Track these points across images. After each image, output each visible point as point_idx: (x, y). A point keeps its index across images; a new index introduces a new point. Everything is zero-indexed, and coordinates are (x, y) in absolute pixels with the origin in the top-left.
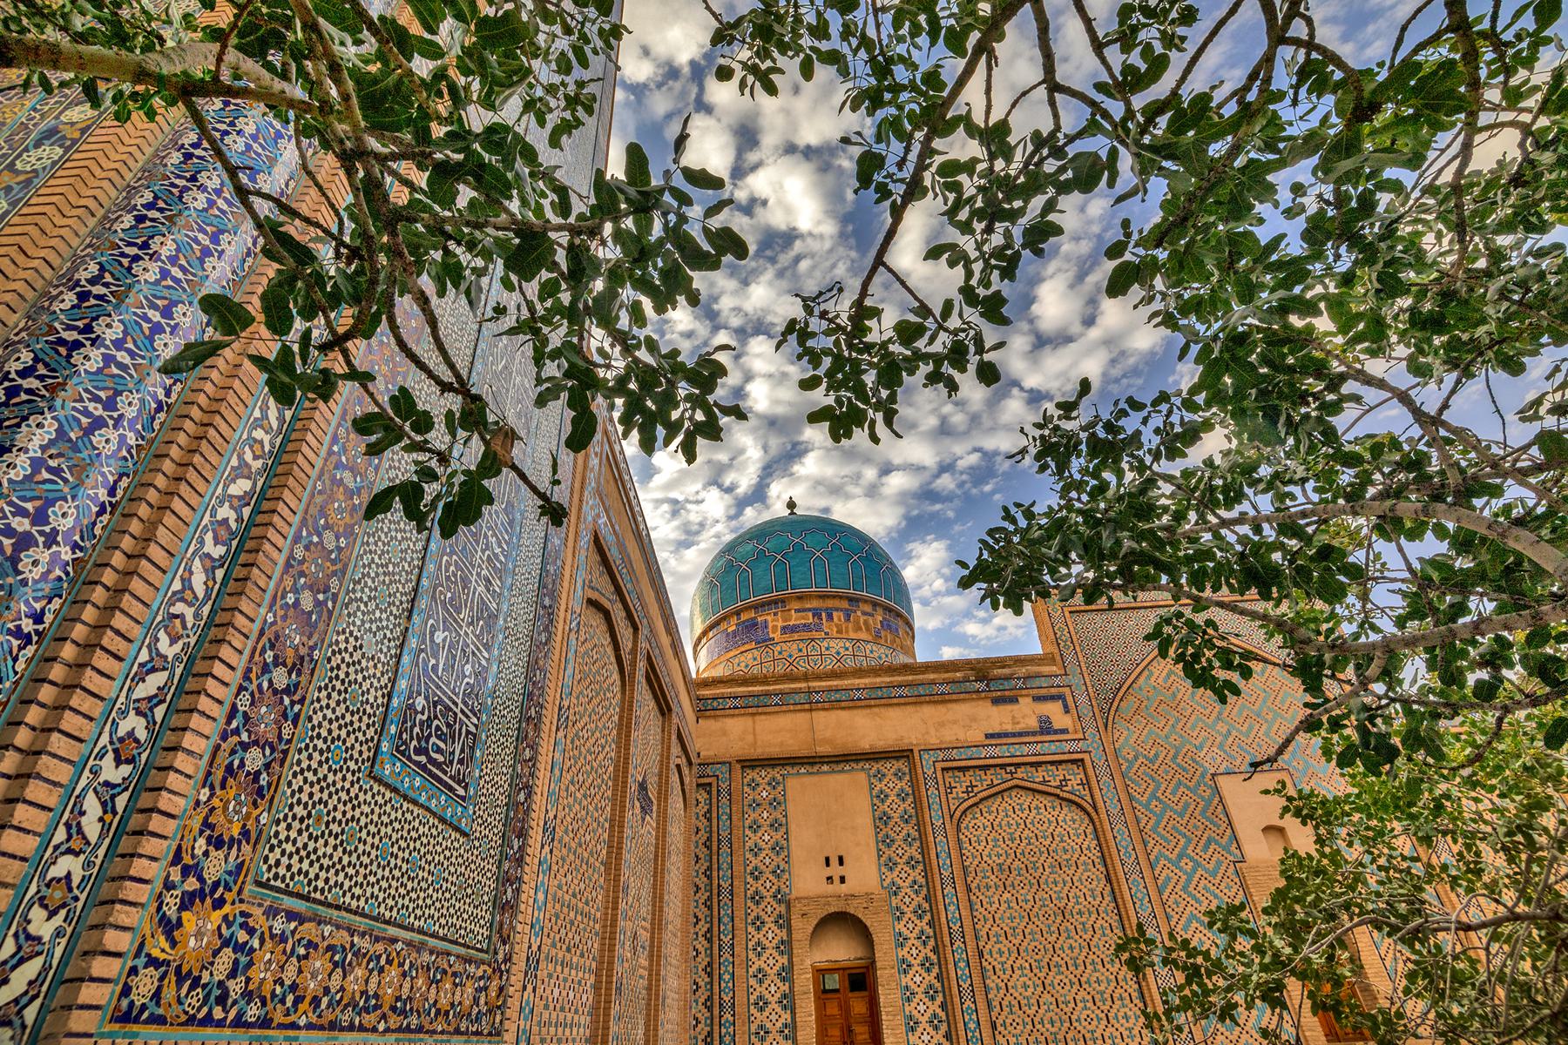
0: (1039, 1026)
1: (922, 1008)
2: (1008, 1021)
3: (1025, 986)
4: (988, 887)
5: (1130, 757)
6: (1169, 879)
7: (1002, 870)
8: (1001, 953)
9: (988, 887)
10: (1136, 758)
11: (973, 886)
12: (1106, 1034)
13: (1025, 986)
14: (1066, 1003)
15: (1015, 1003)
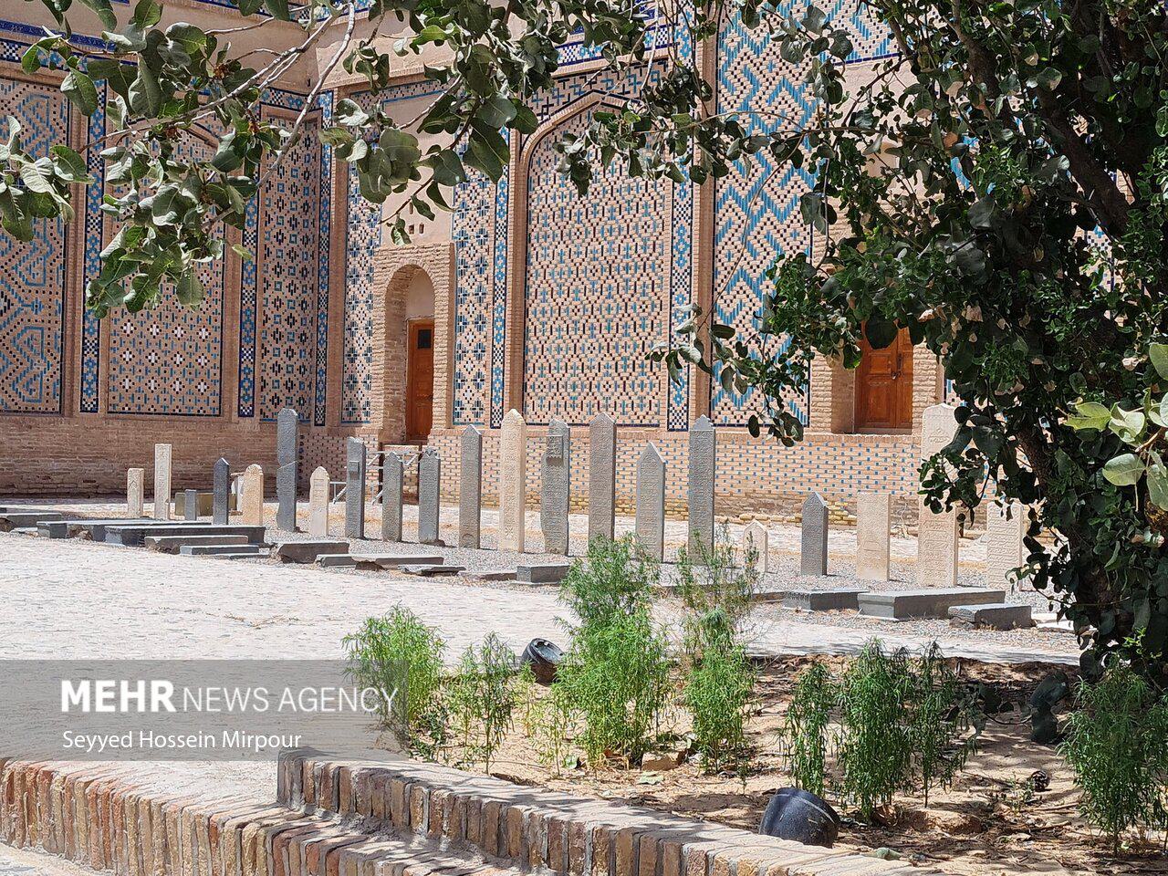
0: (562, 390)
1: (469, 366)
2: (538, 383)
3: (559, 349)
4: (546, 237)
5: (732, 46)
6: (730, 223)
7: (562, 217)
8: (544, 312)
9: (546, 237)
10: (740, 46)
11: (534, 234)
12: (619, 402)
13: (559, 349)
14: (590, 369)
15: (546, 365)
